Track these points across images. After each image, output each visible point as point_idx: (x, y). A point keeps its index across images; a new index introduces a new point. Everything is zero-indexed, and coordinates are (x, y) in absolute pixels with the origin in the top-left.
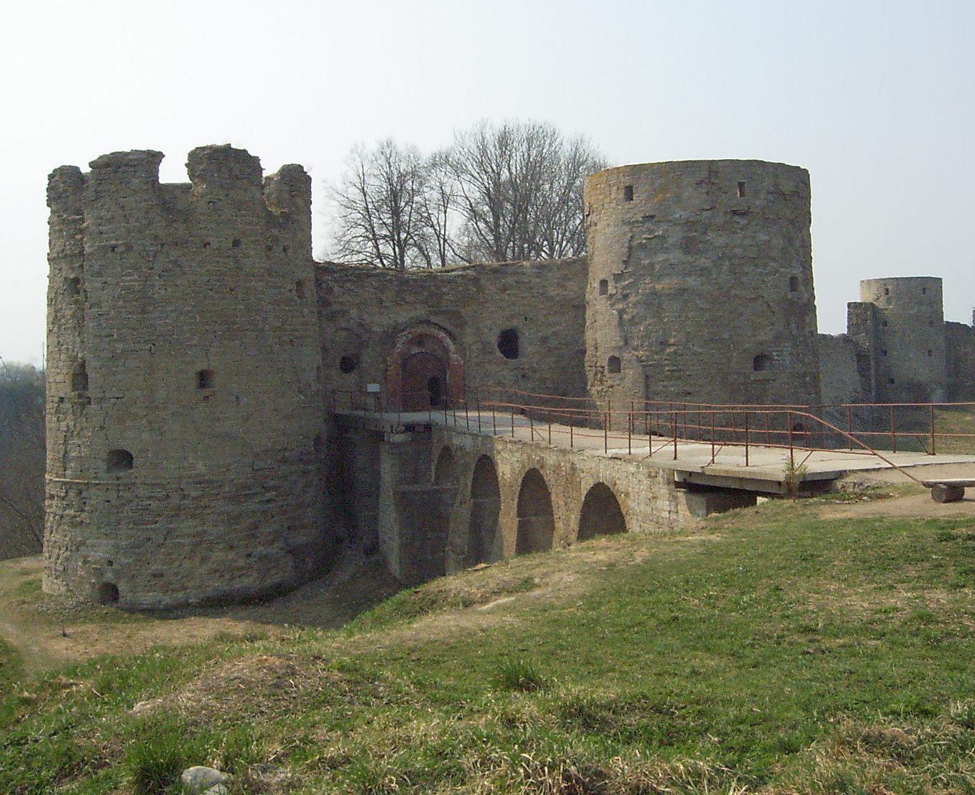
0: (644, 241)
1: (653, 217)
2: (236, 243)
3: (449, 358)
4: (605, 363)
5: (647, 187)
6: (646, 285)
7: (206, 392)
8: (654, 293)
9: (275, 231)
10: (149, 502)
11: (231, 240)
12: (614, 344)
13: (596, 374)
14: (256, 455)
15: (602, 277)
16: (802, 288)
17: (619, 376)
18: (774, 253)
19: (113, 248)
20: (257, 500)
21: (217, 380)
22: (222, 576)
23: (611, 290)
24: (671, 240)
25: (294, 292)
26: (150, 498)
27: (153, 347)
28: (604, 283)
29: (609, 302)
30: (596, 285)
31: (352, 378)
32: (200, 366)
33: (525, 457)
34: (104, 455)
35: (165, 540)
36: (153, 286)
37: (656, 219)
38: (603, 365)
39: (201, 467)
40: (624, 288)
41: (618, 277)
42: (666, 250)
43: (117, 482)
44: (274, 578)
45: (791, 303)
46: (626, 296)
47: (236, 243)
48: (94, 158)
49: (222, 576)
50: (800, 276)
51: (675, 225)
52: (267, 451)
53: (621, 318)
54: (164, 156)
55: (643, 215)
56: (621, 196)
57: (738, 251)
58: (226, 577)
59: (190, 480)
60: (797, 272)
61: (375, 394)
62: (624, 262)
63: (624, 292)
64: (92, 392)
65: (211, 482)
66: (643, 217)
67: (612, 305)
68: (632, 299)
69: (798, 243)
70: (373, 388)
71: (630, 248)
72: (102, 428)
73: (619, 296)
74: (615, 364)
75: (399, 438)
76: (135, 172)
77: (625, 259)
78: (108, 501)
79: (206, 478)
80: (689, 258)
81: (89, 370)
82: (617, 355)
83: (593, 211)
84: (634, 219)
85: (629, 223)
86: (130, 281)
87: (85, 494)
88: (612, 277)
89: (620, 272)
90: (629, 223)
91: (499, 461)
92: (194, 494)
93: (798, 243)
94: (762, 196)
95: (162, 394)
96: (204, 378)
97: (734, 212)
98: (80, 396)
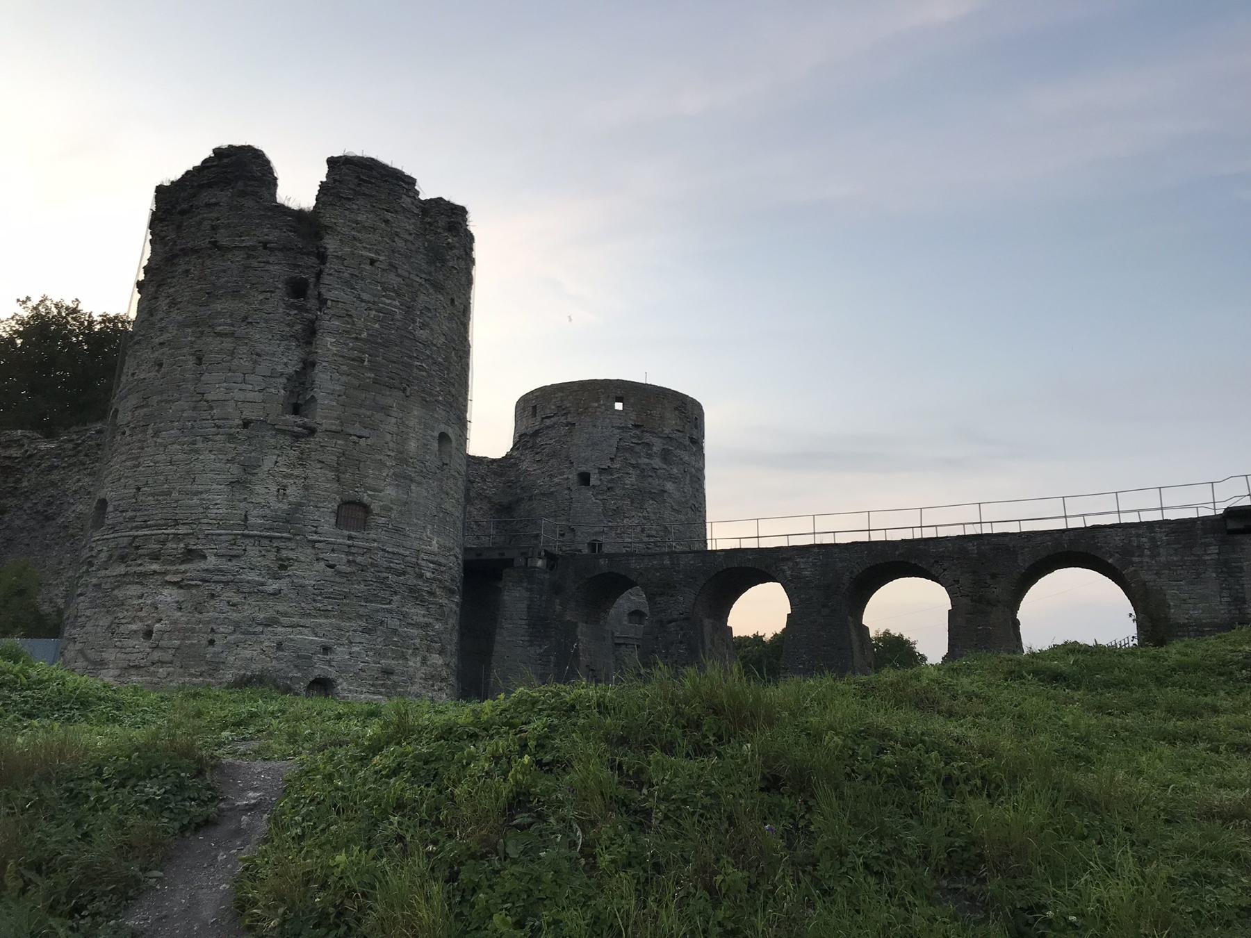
10: (387, 575)
15: (583, 469)
19: (372, 262)
23: (594, 480)
26: (389, 569)
36: (414, 321)
37: (642, 428)
40: (609, 481)
41: (603, 471)
42: (649, 456)
43: (350, 542)
48: (337, 153)
49: (433, 686)
51: (660, 437)
62: (612, 459)
65: (440, 565)
73: (606, 488)
78: (332, 567)
80: (665, 466)
85: (619, 428)
86: (389, 305)
88: (597, 471)
90: (619, 428)
92: (429, 575)
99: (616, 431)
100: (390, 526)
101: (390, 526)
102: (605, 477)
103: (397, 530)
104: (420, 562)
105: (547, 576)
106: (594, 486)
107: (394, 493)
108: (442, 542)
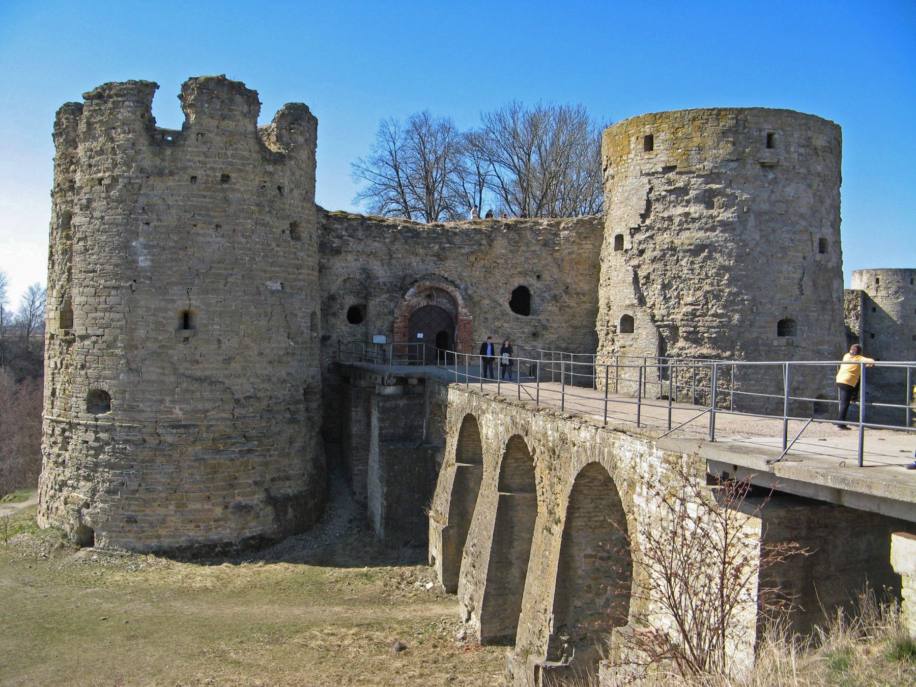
0: (663, 193)
1: (674, 167)
2: (225, 178)
3: (457, 313)
4: (617, 323)
5: (669, 136)
6: (664, 239)
7: (186, 333)
8: (673, 249)
9: (270, 168)
11: (219, 175)
12: (627, 302)
13: (607, 334)
14: (237, 401)
15: (618, 231)
16: (830, 248)
17: (632, 336)
18: (804, 210)
19: (100, 180)
20: (237, 450)
21: (198, 320)
22: (198, 526)
23: (627, 245)
24: (692, 193)
25: (287, 232)
27: (134, 284)
28: (619, 239)
29: (624, 258)
30: (612, 240)
31: (359, 329)
32: (181, 305)
33: (508, 419)
34: (85, 395)
35: (140, 485)
38: (616, 324)
39: (178, 413)
41: (634, 231)
44: (253, 528)
45: (818, 264)
46: (641, 252)
47: (225, 178)
50: (830, 239)
52: (250, 397)
53: (636, 274)
54: (158, 87)
55: (663, 166)
56: (641, 146)
57: (765, 207)
58: (202, 528)
59: (166, 424)
60: (827, 232)
61: (381, 345)
63: (640, 248)
64: (78, 329)
65: (185, 426)
66: (663, 168)
67: (627, 261)
68: (648, 255)
69: (828, 201)
70: (380, 339)
71: (649, 203)
72: (83, 367)
74: (628, 324)
75: (390, 390)
76: (124, 102)
77: (643, 212)
79: (183, 423)
81: (74, 307)
82: (630, 313)
83: (610, 164)
84: (653, 170)
85: (648, 174)
87: (67, 434)
88: (629, 231)
89: (637, 226)
90: (648, 174)
91: (483, 422)
93: (828, 201)
94: (792, 149)
95: (141, 333)
96: (186, 320)
97: (763, 165)
98: (67, 334)
99: (645, 180)
100: (125, 406)
101: (125, 406)
102: (640, 237)
103: (132, 408)
104: (160, 431)
105: (402, 403)
106: (626, 251)
107: (126, 378)
108: (187, 407)
